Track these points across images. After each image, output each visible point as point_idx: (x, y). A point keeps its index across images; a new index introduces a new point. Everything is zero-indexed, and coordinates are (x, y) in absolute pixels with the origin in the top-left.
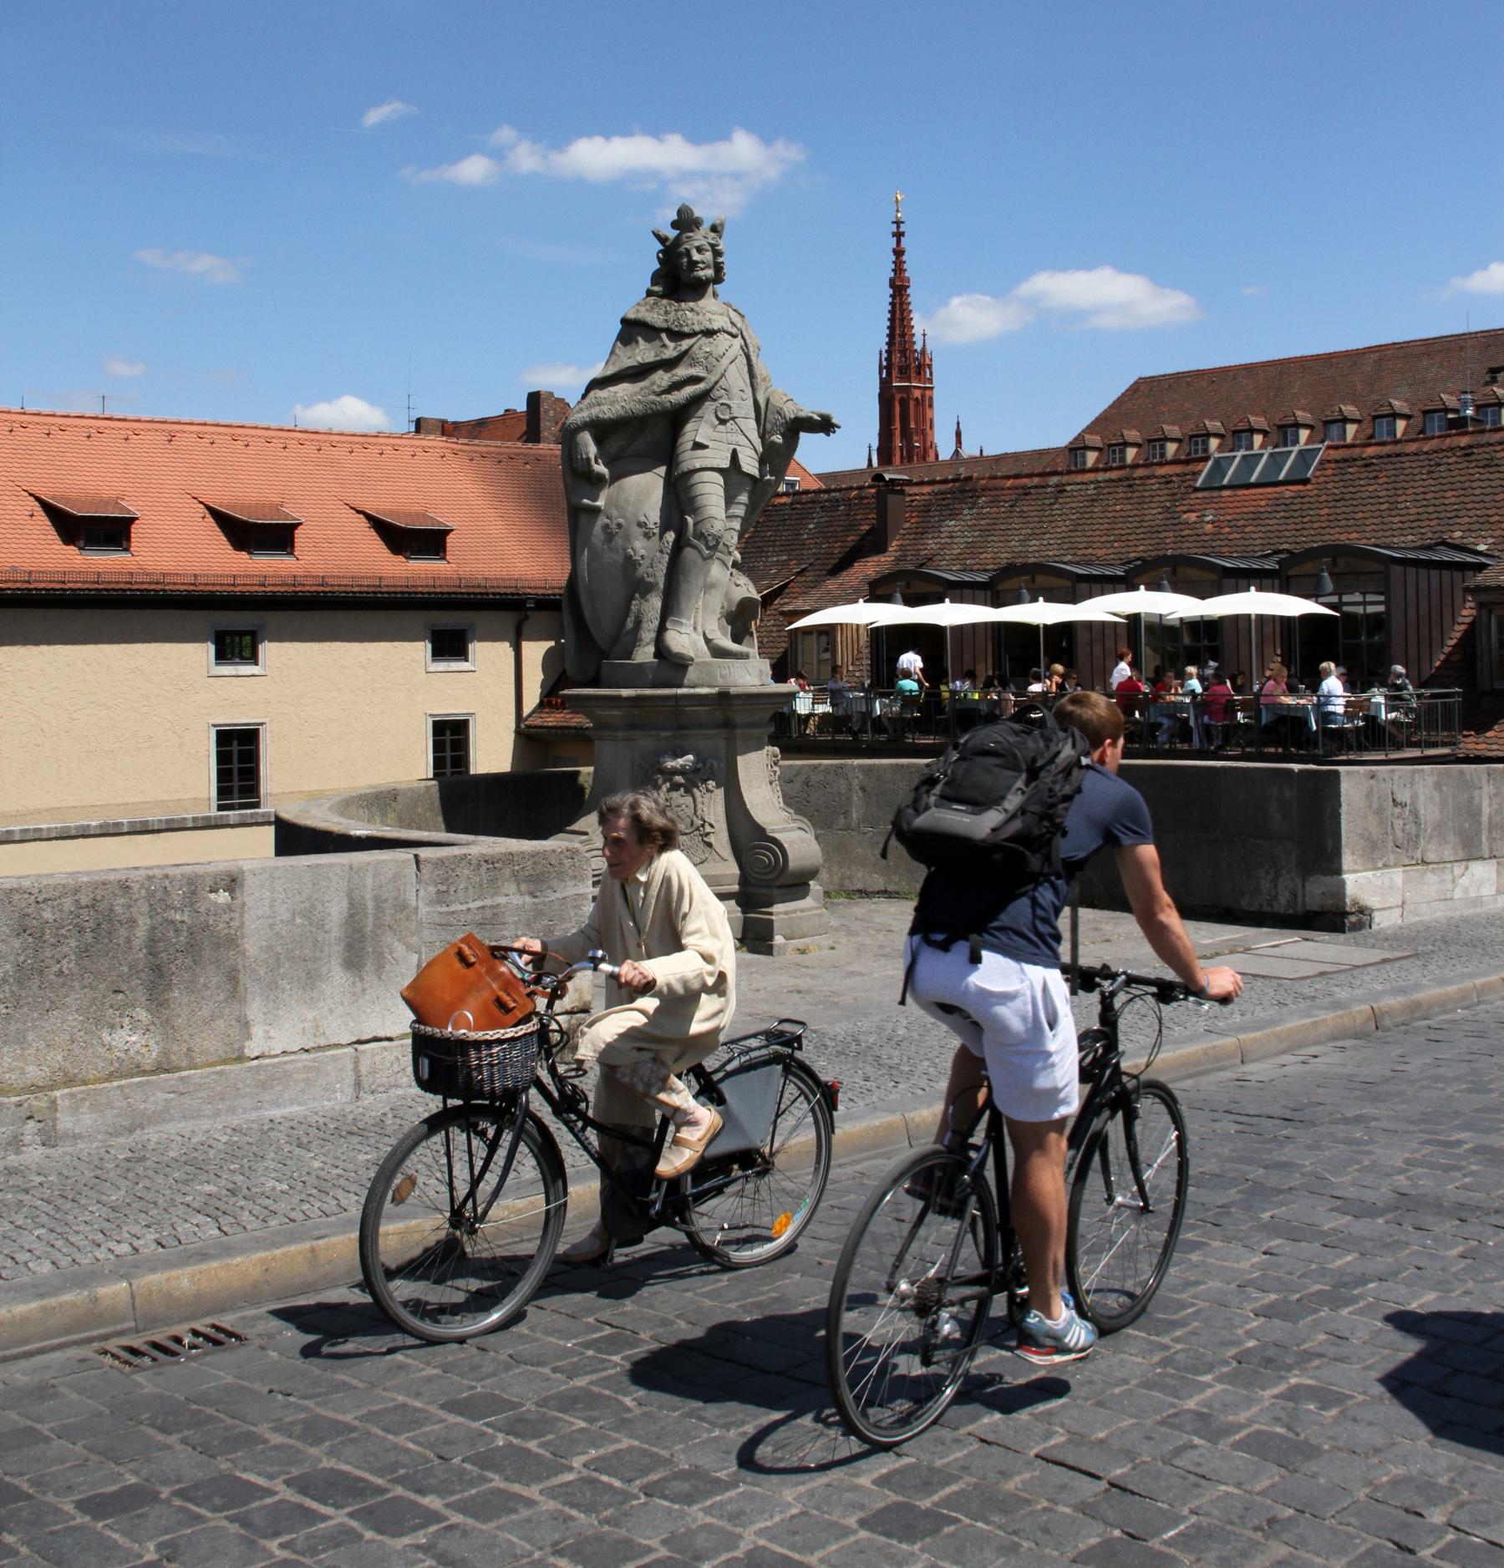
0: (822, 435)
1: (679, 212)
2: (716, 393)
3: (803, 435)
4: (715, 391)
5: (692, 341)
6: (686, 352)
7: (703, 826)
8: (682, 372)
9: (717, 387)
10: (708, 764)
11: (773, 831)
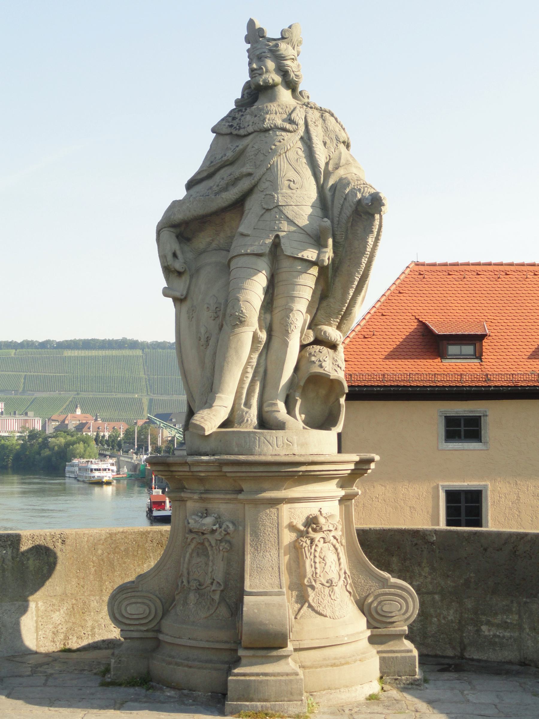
2: (263, 185)
6: (242, 152)
7: (212, 583)
9: (263, 180)
10: (224, 526)
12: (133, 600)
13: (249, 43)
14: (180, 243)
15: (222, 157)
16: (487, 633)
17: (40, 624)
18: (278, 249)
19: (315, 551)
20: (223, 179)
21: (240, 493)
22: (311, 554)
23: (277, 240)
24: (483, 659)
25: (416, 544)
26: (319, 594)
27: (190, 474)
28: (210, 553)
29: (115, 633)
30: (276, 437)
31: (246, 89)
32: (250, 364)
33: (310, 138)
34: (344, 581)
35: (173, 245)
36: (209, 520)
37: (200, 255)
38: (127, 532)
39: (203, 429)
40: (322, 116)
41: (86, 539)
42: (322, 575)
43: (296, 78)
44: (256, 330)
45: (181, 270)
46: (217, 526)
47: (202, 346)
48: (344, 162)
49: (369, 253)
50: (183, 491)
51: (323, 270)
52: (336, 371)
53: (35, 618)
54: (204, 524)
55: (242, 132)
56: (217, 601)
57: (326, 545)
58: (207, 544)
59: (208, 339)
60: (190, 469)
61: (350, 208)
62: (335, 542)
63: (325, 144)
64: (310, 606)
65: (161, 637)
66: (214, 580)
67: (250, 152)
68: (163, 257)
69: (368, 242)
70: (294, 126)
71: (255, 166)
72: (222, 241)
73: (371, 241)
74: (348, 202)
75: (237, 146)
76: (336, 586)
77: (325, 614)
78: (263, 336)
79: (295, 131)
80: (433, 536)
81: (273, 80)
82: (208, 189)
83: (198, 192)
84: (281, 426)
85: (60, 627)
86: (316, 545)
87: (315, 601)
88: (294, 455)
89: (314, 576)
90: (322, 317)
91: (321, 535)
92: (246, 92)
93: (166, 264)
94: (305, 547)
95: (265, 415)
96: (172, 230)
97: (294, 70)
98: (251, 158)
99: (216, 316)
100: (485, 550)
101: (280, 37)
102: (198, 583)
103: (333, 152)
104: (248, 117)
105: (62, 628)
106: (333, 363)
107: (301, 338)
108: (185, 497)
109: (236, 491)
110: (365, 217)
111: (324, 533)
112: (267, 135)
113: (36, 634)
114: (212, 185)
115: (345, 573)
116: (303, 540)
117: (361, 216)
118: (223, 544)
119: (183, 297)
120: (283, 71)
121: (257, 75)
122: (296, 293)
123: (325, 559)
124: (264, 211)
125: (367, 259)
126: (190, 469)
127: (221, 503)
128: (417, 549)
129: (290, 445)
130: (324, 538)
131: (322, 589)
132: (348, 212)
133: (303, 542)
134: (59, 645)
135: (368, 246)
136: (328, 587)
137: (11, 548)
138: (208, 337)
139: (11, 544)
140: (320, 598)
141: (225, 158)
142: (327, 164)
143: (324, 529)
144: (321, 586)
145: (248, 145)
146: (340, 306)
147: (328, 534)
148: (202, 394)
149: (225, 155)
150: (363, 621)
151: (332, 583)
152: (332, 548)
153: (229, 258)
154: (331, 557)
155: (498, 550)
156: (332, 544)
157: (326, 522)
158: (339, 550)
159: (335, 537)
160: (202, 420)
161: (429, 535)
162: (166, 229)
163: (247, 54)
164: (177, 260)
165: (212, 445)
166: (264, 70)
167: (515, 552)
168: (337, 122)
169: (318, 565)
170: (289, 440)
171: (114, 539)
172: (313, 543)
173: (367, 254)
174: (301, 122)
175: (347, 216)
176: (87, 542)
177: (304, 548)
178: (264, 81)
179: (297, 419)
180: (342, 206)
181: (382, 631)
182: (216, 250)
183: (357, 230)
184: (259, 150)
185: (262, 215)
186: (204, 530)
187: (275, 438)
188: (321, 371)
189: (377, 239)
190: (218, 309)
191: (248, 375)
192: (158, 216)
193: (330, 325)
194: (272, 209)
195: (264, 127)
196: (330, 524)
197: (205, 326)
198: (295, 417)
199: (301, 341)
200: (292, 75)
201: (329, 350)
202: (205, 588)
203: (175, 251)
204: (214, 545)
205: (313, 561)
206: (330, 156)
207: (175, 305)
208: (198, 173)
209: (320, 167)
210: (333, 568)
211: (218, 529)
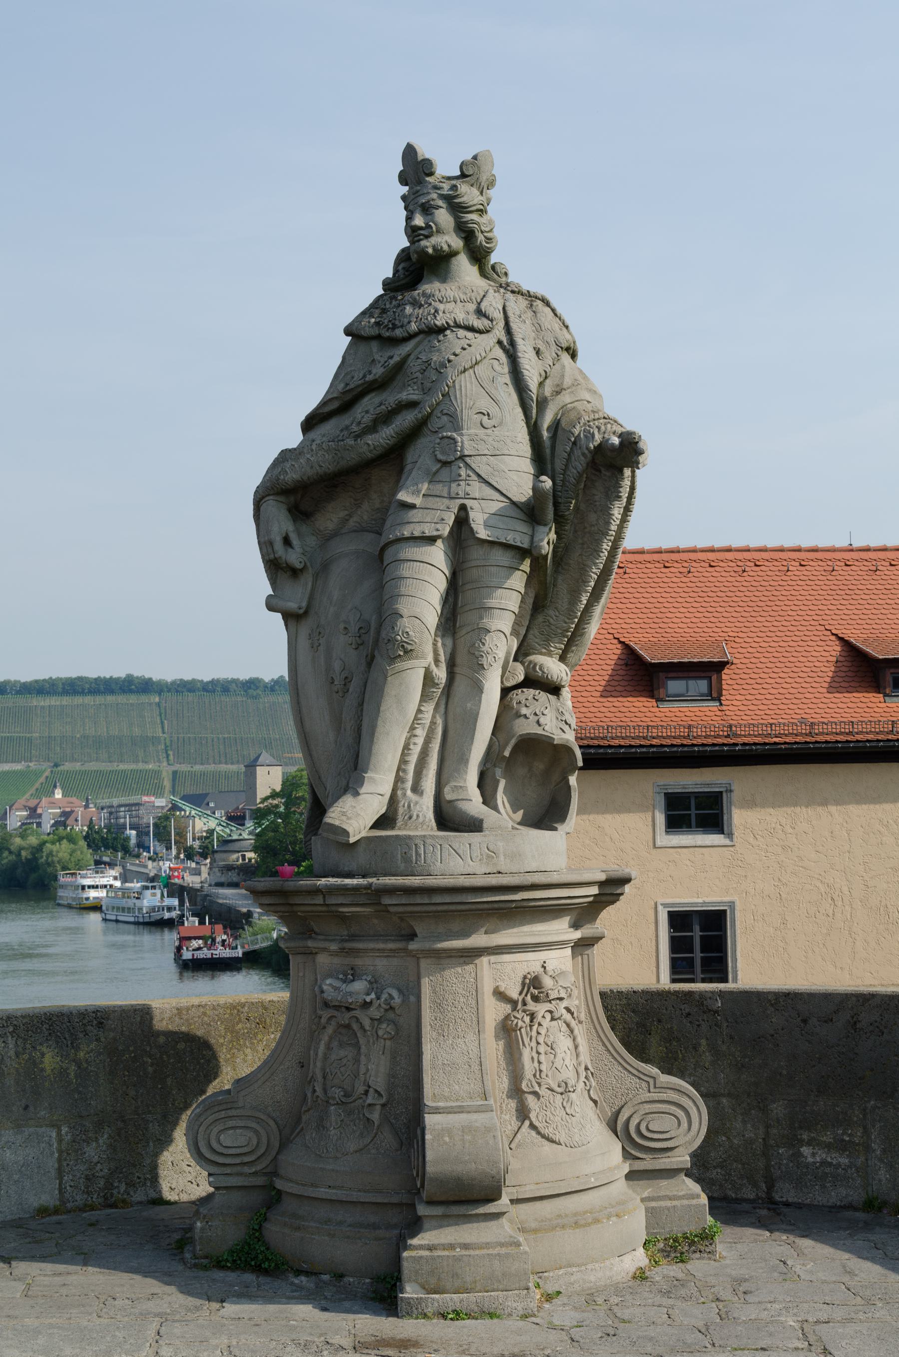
1: (475, 158)
2: (434, 424)
4: (434, 419)
6: (400, 366)
7: (366, 1093)
8: (391, 398)
9: (437, 413)
10: (384, 996)
12: (231, 1123)
13: (406, 185)
14: (294, 521)
15: (364, 376)
16: (810, 1160)
17: (65, 1164)
18: (463, 528)
19: (538, 1033)
20: (367, 412)
21: (413, 940)
22: (531, 1040)
23: (462, 514)
24: (805, 1202)
25: (689, 1014)
26: (546, 1106)
27: (324, 909)
28: (362, 1041)
29: (189, 1175)
30: (470, 844)
31: (402, 262)
32: (419, 722)
33: (512, 343)
34: (584, 1082)
35: (282, 523)
36: (359, 986)
37: (328, 540)
38: (206, 1005)
39: (346, 833)
40: (531, 305)
41: (139, 1019)
42: (550, 1075)
43: (487, 243)
44: (430, 663)
45: (299, 566)
46: (373, 996)
47: (337, 692)
48: (570, 383)
49: (614, 533)
50: (310, 938)
51: (538, 562)
52: (564, 731)
53: (56, 1155)
54: (351, 994)
55: (398, 333)
56: (376, 1123)
57: (554, 1023)
58: (355, 1026)
59: (347, 681)
60: (324, 901)
61: (583, 458)
62: (568, 1016)
63: (538, 352)
64: (533, 1126)
65: (279, 1184)
66: (369, 1087)
67: (414, 366)
68: (265, 545)
69: (613, 515)
70: (486, 322)
71: (423, 390)
72: (365, 517)
73: (617, 513)
74: (580, 448)
75: (391, 357)
76: (573, 1092)
77: (557, 1141)
78: (441, 674)
79: (488, 331)
80: (717, 1000)
81: (449, 246)
82: (342, 431)
83: (324, 436)
84: (474, 826)
85: (99, 1166)
86: (540, 1024)
87: (540, 1119)
88: (500, 873)
89: (538, 1076)
90: (537, 640)
91: (548, 1006)
92: (400, 267)
93: (272, 556)
94: (521, 1028)
95: (446, 808)
96: (282, 498)
97: (483, 228)
98: (415, 376)
100: (805, 1021)
101: (458, 173)
102: (342, 1093)
103: (552, 365)
104: (408, 309)
105: (101, 1170)
106: (557, 718)
107: (502, 677)
108: (315, 948)
109: (402, 936)
110: (608, 474)
111: (551, 1003)
112: (441, 337)
113: (58, 1181)
114: (347, 422)
115: (586, 1069)
116: (518, 1016)
117: (600, 471)
118: (384, 1026)
119: (301, 611)
120: (464, 231)
121: (421, 237)
122: (492, 602)
123: (554, 1046)
124: (439, 465)
125: (610, 544)
127: (378, 956)
128: (690, 1022)
129: (493, 857)
130: (551, 1012)
131: (551, 1097)
132: (579, 463)
133: (518, 1019)
134: (98, 1198)
135: (612, 522)
136: (562, 1094)
137: (15, 1038)
138: (346, 678)
139: (13, 1032)
140: (548, 1113)
141: (369, 378)
142: (541, 384)
143: (551, 997)
144: (549, 1092)
146: (566, 623)
147: (558, 1004)
148: (339, 774)
149: (370, 372)
150: (616, 1148)
151: (567, 1086)
152: (564, 1028)
153: (382, 544)
154: (564, 1043)
155: (826, 1022)
156: (565, 1022)
157: (554, 985)
158: (576, 1032)
159: (568, 1010)
160: (344, 818)
161: (710, 998)
162: (271, 497)
163: (403, 204)
164: (290, 550)
165: (362, 859)
166: (434, 229)
167: (855, 1023)
168: (556, 315)
169: (542, 1058)
170: (491, 848)
171: (185, 1017)
172: (535, 1020)
173: (612, 535)
174: (498, 316)
175: (578, 472)
176: (140, 1023)
177: (520, 1030)
178: (434, 248)
179: (499, 812)
180: (569, 455)
181: (648, 1163)
182: (355, 531)
183: (594, 495)
184: (428, 363)
185: (437, 471)
186: (351, 1004)
187: (468, 846)
188: (539, 731)
189: (627, 510)
190: (362, 631)
191: (416, 740)
192: (256, 476)
193: (549, 654)
194: (453, 461)
195: (435, 325)
196: (560, 988)
197: (341, 659)
198: (495, 808)
199: (502, 682)
200: (481, 238)
201: (550, 696)
202: (354, 1101)
203: (287, 534)
204: (367, 1028)
205: (534, 1050)
206: (546, 372)
207: (286, 625)
208: (324, 403)
209: (531, 391)
210: (567, 1062)
211: (374, 1001)
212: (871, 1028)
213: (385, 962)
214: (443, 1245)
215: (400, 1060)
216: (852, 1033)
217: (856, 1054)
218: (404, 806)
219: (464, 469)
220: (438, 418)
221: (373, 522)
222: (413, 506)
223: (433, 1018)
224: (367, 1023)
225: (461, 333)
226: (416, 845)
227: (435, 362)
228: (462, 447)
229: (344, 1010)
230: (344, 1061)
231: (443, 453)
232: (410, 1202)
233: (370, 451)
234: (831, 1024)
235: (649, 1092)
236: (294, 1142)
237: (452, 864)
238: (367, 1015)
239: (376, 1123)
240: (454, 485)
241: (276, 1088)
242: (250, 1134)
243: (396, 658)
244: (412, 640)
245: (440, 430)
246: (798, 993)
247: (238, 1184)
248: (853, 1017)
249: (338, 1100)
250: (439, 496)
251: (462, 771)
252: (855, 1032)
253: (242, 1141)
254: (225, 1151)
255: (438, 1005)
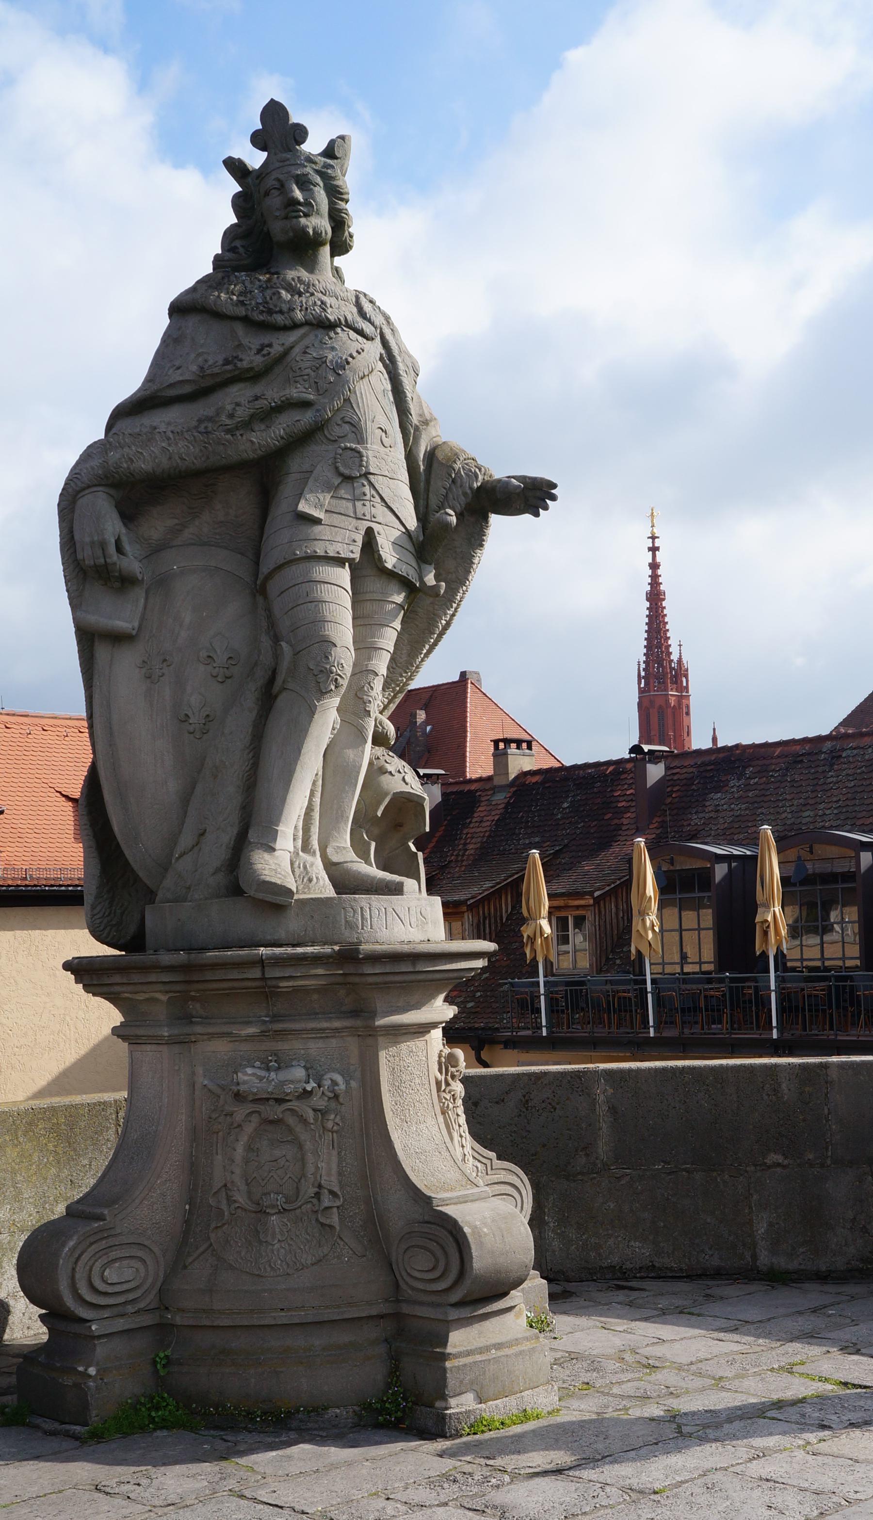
0: (527, 517)
3: (495, 520)
5: (292, 337)
7: (318, 1195)
10: (327, 1083)
11: (446, 1202)
28: (304, 1136)
31: (237, 238)
58: (291, 1120)
60: (263, 974)
66: (320, 1186)
99: (228, 674)
126: (263, 974)
138: (208, 716)
145: (292, 348)
167: (527, 1101)
184: (322, 360)
187: (384, 910)
190: (230, 662)
212: (544, 1105)
213: (320, 1044)
214: (480, 1348)
215: (345, 1154)
216: (524, 1112)
217: (529, 1131)
218: (300, 868)
219: (367, 487)
220: (338, 425)
221: (218, 537)
222: (317, 521)
223: (393, 1103)
224: (310, 1115)
225: (351, 333)
226: (362, 908)
227: (331, 361)
228: (367, 462)
229: (271, 1102)
230: (282, 1162)
231: (346, 466)
232: (392, 1312)
233: (254, 451)
234: (502, 1104)
235: (487, 1174)
236: (189, 1267)
237: (396, 930)
238: (310, 1107)
239: (338, 1228)
240: (359, 504)
241: (155, 1207)
242: (138, 1265)
243: (326, 693)
244: (345, 674)
245: (340, 439)
246: (469, 1076)
247: (125, 1328)
248: (524, 1096)
249: (280, 1208)
250: (344, 515)
251: (342, 830)
252: (527, 1110)
253: (128, 1274)
254: (110, 1289)
255: (397, 1088)
